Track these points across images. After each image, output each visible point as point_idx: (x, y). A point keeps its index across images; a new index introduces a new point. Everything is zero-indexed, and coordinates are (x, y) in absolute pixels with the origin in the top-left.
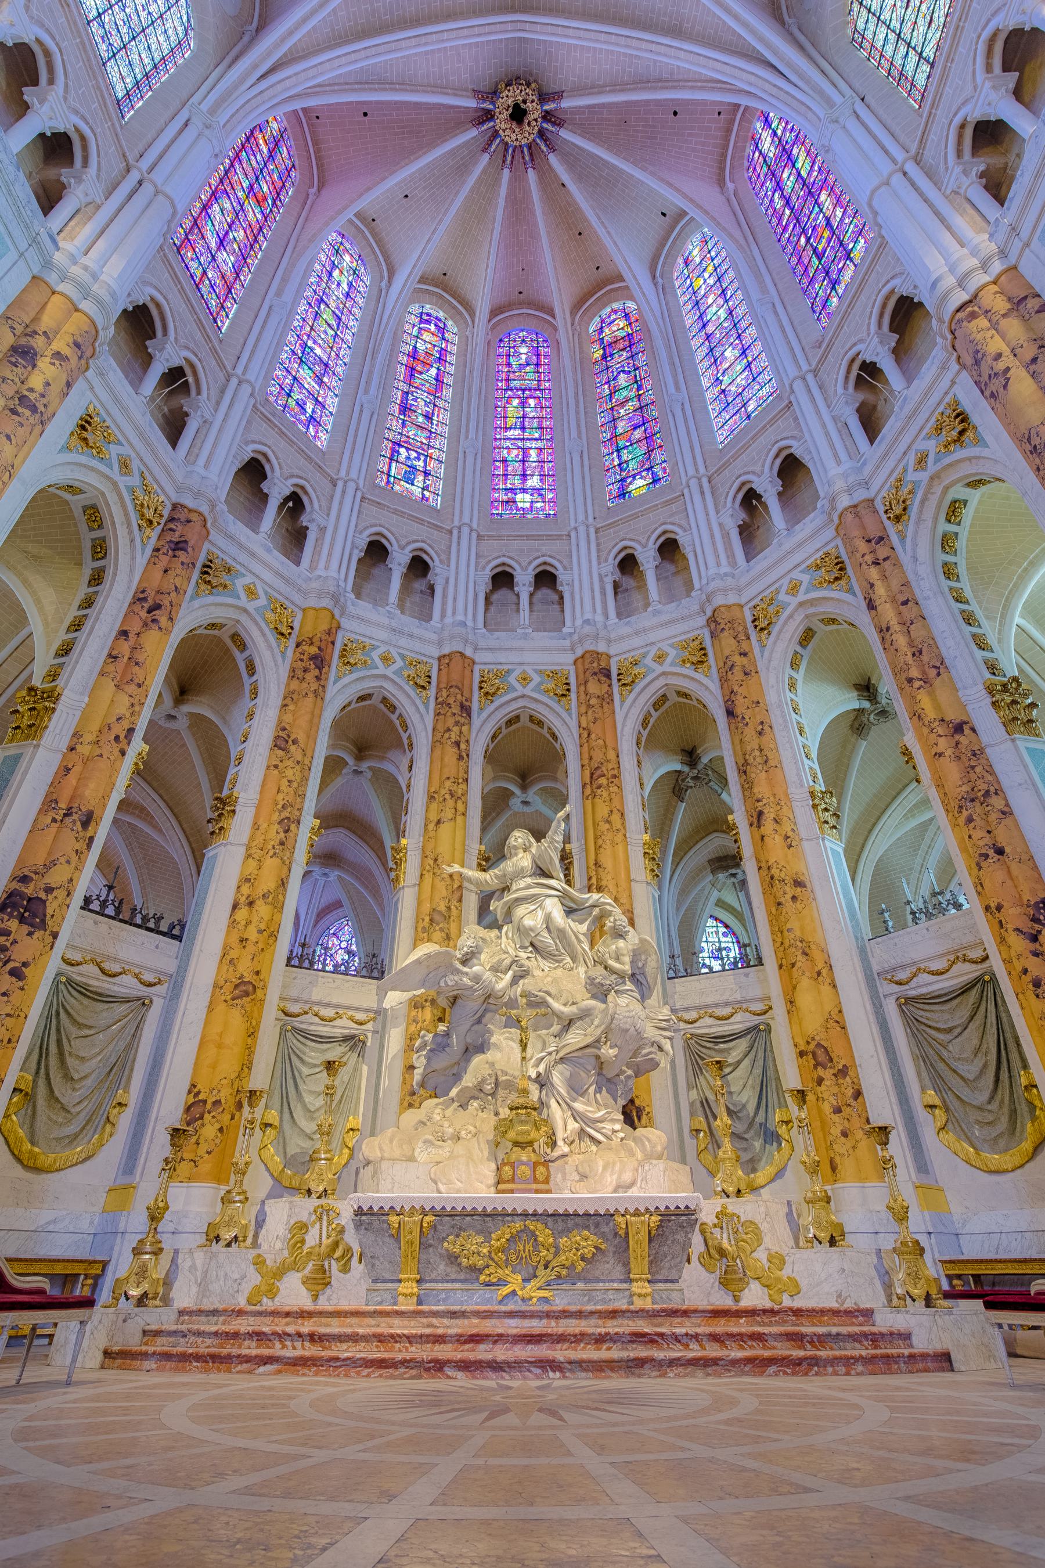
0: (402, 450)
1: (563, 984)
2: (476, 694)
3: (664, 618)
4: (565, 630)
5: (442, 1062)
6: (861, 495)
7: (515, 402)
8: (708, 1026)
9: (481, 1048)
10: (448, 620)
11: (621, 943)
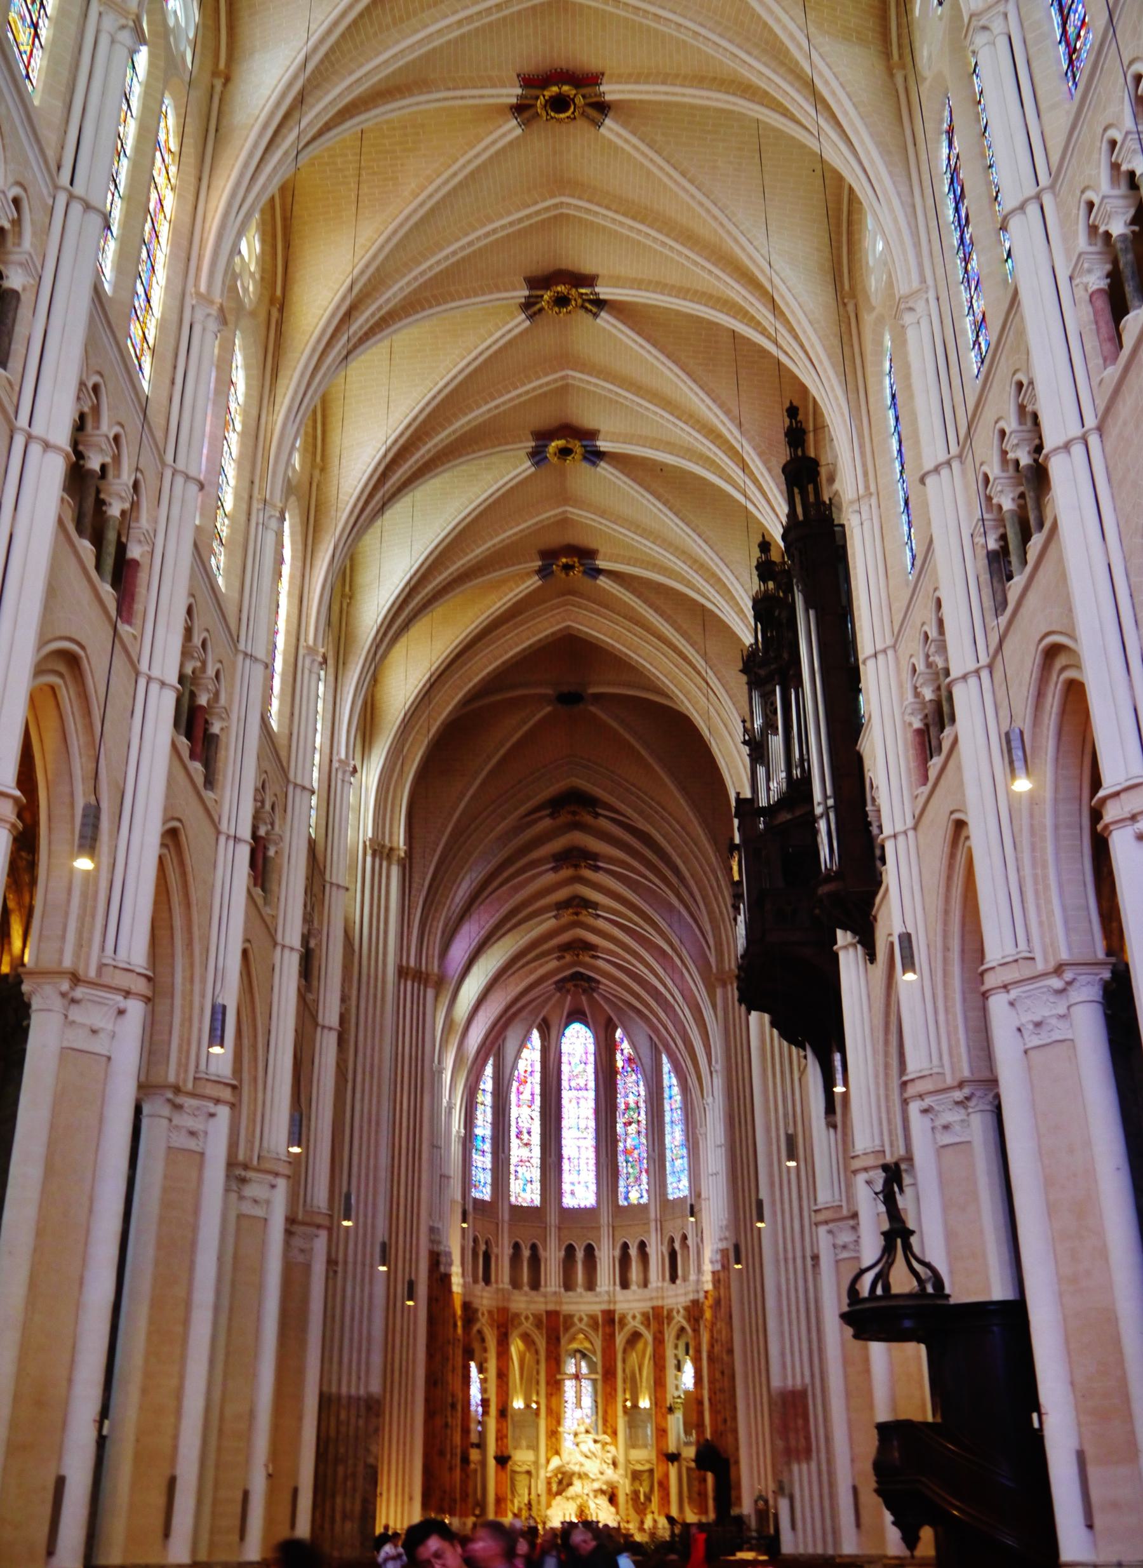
0: (519, 1169)
1: (592, 1467)
2: (562, 1329)
3: (637, 1297)
4: (598, 1289)
5: (561, 1487)
6: (696, 1297)
7: (574, 1102)
8: (639, 1467)
9: (570, 1484)
10: (549, 1289)
11: (609, 1455)
